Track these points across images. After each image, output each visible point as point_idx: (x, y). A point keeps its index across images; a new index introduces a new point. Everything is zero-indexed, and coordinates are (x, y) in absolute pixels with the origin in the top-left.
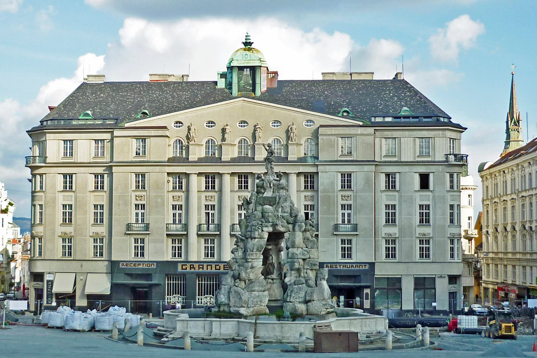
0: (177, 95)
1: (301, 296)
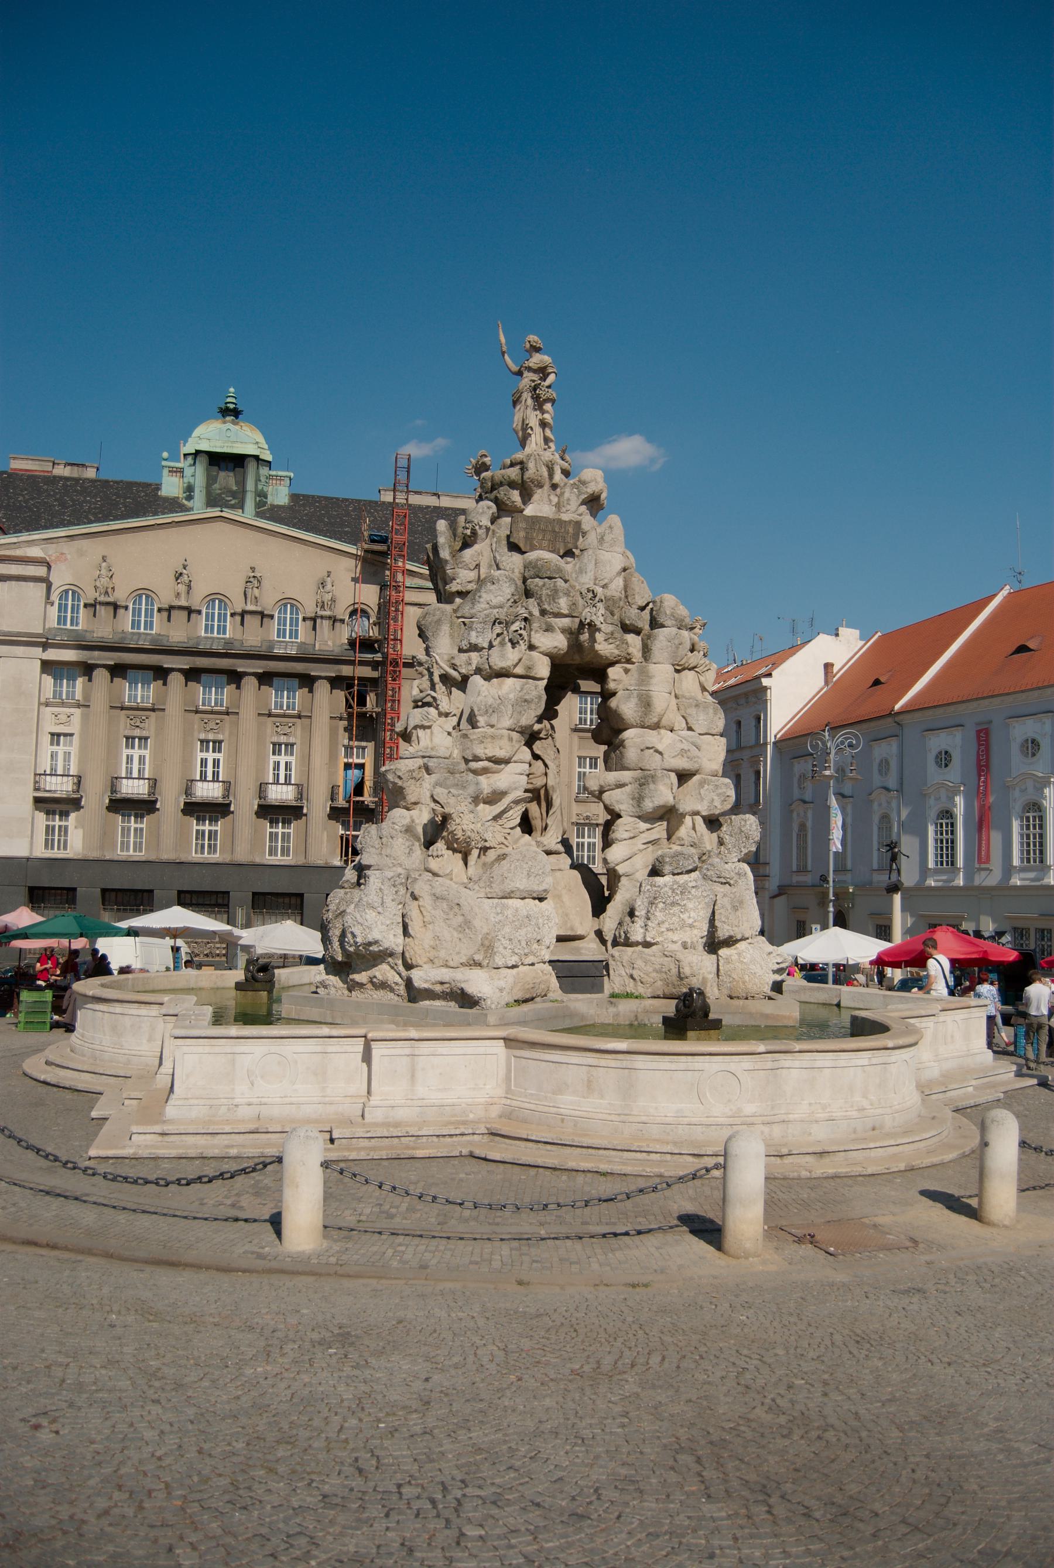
0: (73, 501)
1: (690, 921)
